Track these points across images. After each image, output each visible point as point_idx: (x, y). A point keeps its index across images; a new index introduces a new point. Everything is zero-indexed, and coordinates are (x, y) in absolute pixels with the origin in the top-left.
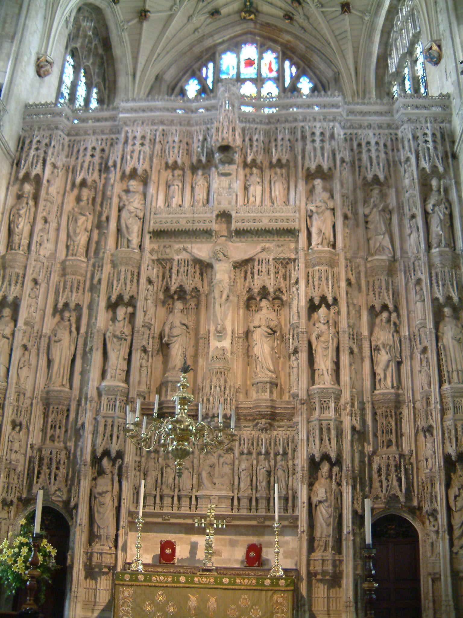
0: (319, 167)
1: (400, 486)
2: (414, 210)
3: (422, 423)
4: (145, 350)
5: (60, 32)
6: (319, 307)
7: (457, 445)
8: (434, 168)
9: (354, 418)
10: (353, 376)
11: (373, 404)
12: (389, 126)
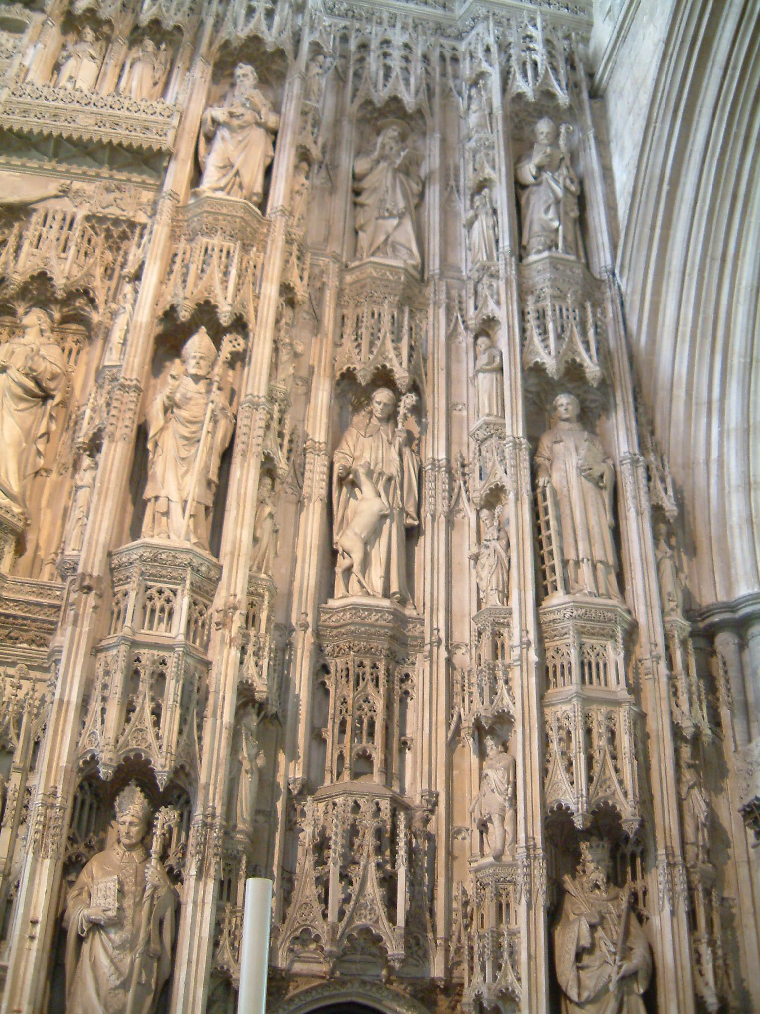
1: (391, 903)
7: (590, 779)
9: (250, 660)
10: (266, 536)
11: (317, 634)
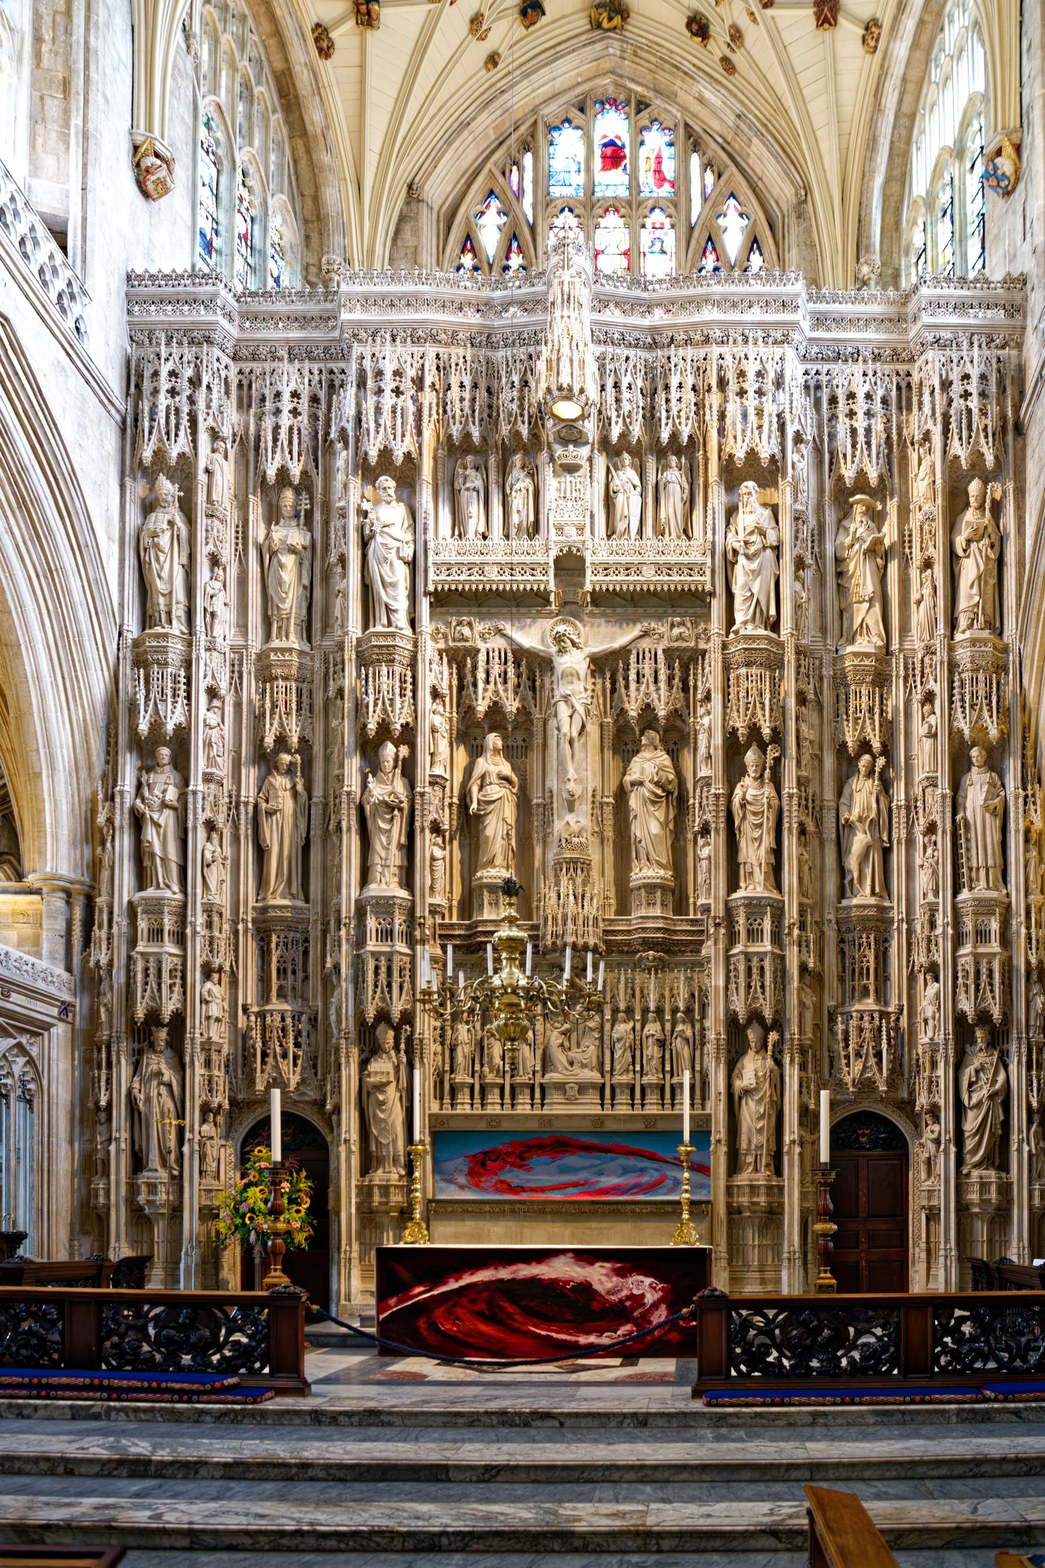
0: (752, 455)
1: (879, 1063)
2: (931, 549)
3: (920, 959)
4: (436, 828)
5: (175, 65)
6: (747, 746)
7: (976, 998)
8: (978, 456)
11: (838, 922)
12: (895, 356)
